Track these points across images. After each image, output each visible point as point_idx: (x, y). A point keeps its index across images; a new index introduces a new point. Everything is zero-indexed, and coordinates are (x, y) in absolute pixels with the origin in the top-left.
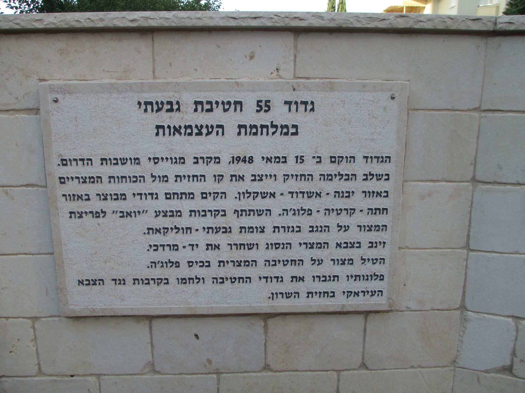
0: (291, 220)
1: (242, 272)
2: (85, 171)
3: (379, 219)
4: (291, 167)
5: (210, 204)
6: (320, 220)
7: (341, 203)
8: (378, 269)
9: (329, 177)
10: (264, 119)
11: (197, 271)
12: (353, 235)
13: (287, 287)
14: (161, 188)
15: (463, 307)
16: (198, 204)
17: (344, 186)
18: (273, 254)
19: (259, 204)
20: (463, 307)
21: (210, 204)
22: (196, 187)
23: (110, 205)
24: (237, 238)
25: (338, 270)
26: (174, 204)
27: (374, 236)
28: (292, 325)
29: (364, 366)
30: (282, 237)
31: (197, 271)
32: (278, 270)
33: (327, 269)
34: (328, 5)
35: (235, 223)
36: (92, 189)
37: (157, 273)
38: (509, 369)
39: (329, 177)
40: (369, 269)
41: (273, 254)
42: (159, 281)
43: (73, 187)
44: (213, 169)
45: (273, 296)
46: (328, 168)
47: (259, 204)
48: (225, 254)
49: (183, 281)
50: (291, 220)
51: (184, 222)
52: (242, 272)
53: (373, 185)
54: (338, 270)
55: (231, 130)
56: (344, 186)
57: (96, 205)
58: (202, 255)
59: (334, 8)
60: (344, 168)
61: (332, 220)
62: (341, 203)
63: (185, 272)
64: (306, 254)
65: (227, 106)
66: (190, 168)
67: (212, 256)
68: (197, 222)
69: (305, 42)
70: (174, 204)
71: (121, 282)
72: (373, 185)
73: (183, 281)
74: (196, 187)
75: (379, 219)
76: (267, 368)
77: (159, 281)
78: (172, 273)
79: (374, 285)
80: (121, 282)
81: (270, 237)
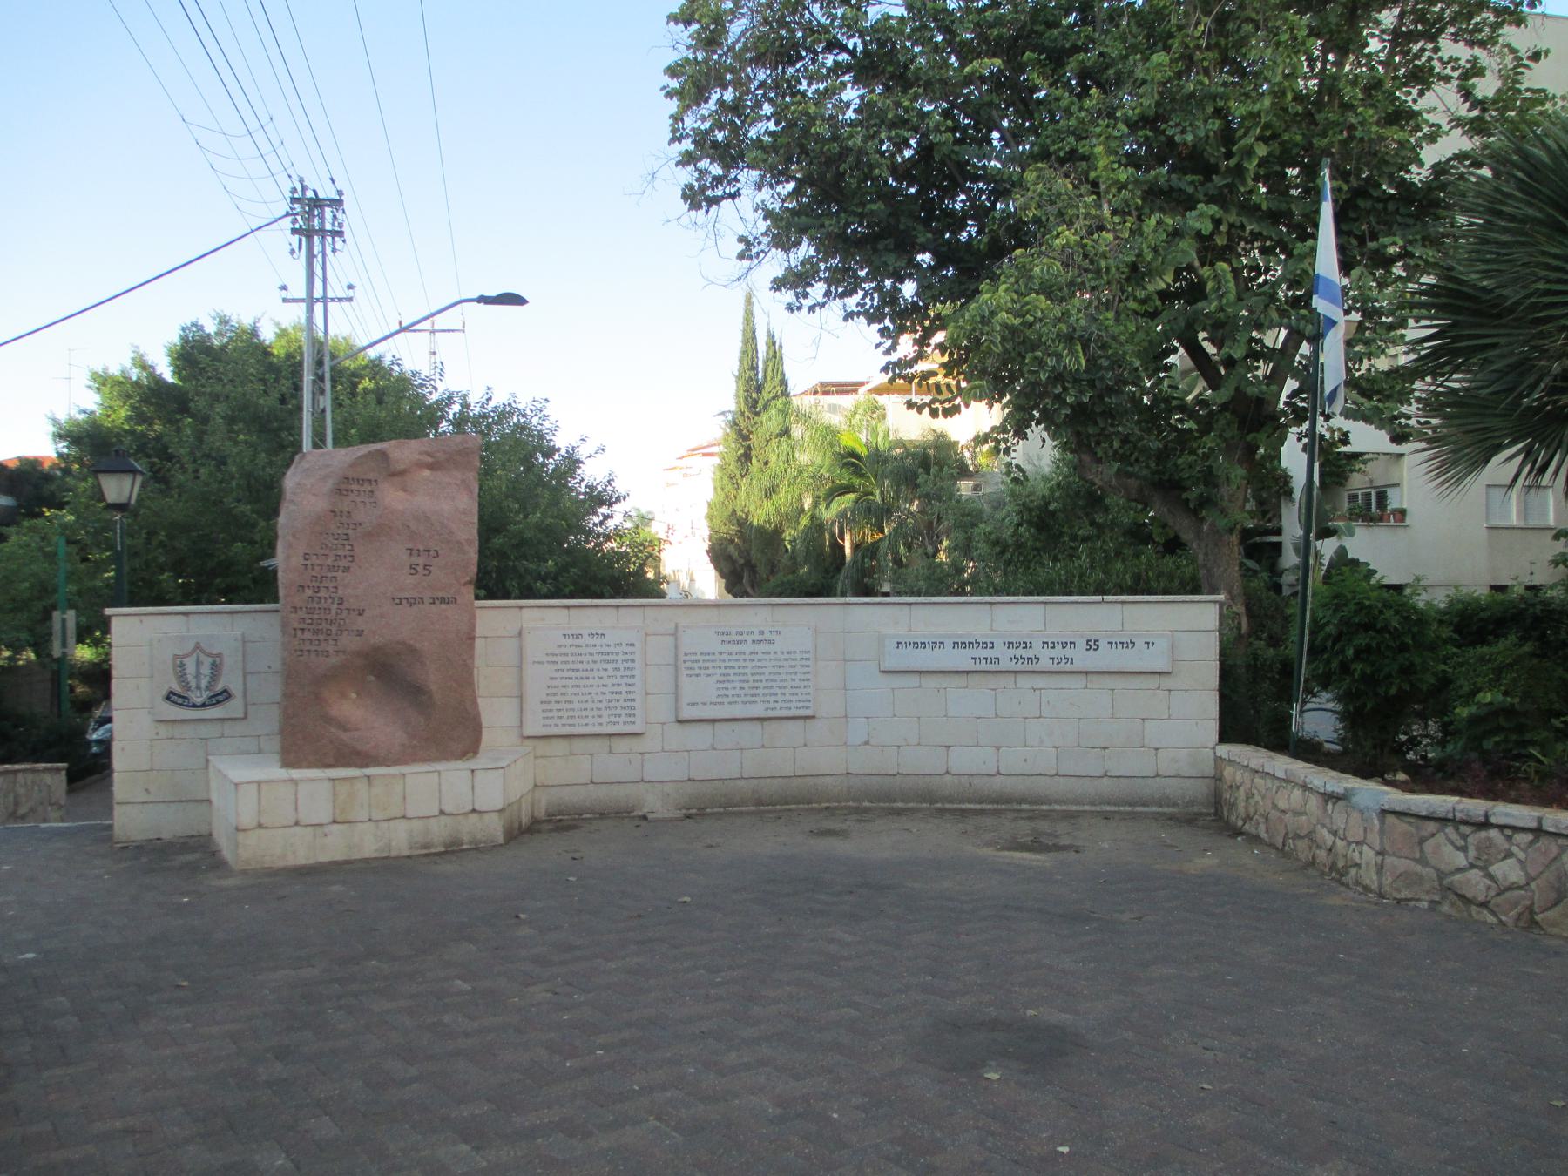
0: (772, 677)
1: (753, 699)
2: (693, 658)
3: (808, 676)
4: (772, 656)
5: (741, 671)
6: (784, 677)
7: (792, 670)
8: (808, 697)
9: (786, 660)
10: (762, 637)
11: (736, 699)
12: (797, 683)
13: (772, 705)
14: (723, 665)
15: (846, 716)
16: (736, 671)
17: (793, 663)
18: (766, 691)
19: (760, 670)
20: (846, 716)
21: (741, 671)
22: (736, 664)
23: (703, 672)
24: (751, 684)
25: (792, 698)
26: (728, 671)
27: (806, 683)
28: (774, 724)
29: (805, 745)
30: (769, 684)
31: (736, 699)
32: (768, 698)
33: (788, 697)
34: (741, 362)
35: (751, 678)
36: (695, 665)
37: (719, 700)
38: (867, 743)
39: (786, 660)
40: (804, 697)
41: (766, 691)
42: (721, 703)
43: (689, 664)
44: (743, 657)
45: (766, 709)
46: (786, 656)
47: (760, 670)
48: (747, 691)
49: (730, 703)
50: (772, 677)
51: (731, 678)
52: (753, 699)
53: (804, 662)
54: (792, 698)
55: (749, 642)
56: (793, 663)
57: (697, 672)
58: (738, 691)
59: (754, 369)
60: (792, 656)
61: (789, 677)
62: (792, 670)
63: (731, 699)
64: (779, 691)
65: (748, 633)
66: (734, 657)
67: (742, 692)
68: (737, 678)
69: (776, 608)
70: (728, 671)
71: (704, 704)
72: (804, 662)
73: (730, 703)
74: (736, 664)
75: (808, 676)
76: (763, 746)
77: (721, 703)
78: (726, 700)
79: (807, 704)
80: (704, 704)
81: (764, 684)
